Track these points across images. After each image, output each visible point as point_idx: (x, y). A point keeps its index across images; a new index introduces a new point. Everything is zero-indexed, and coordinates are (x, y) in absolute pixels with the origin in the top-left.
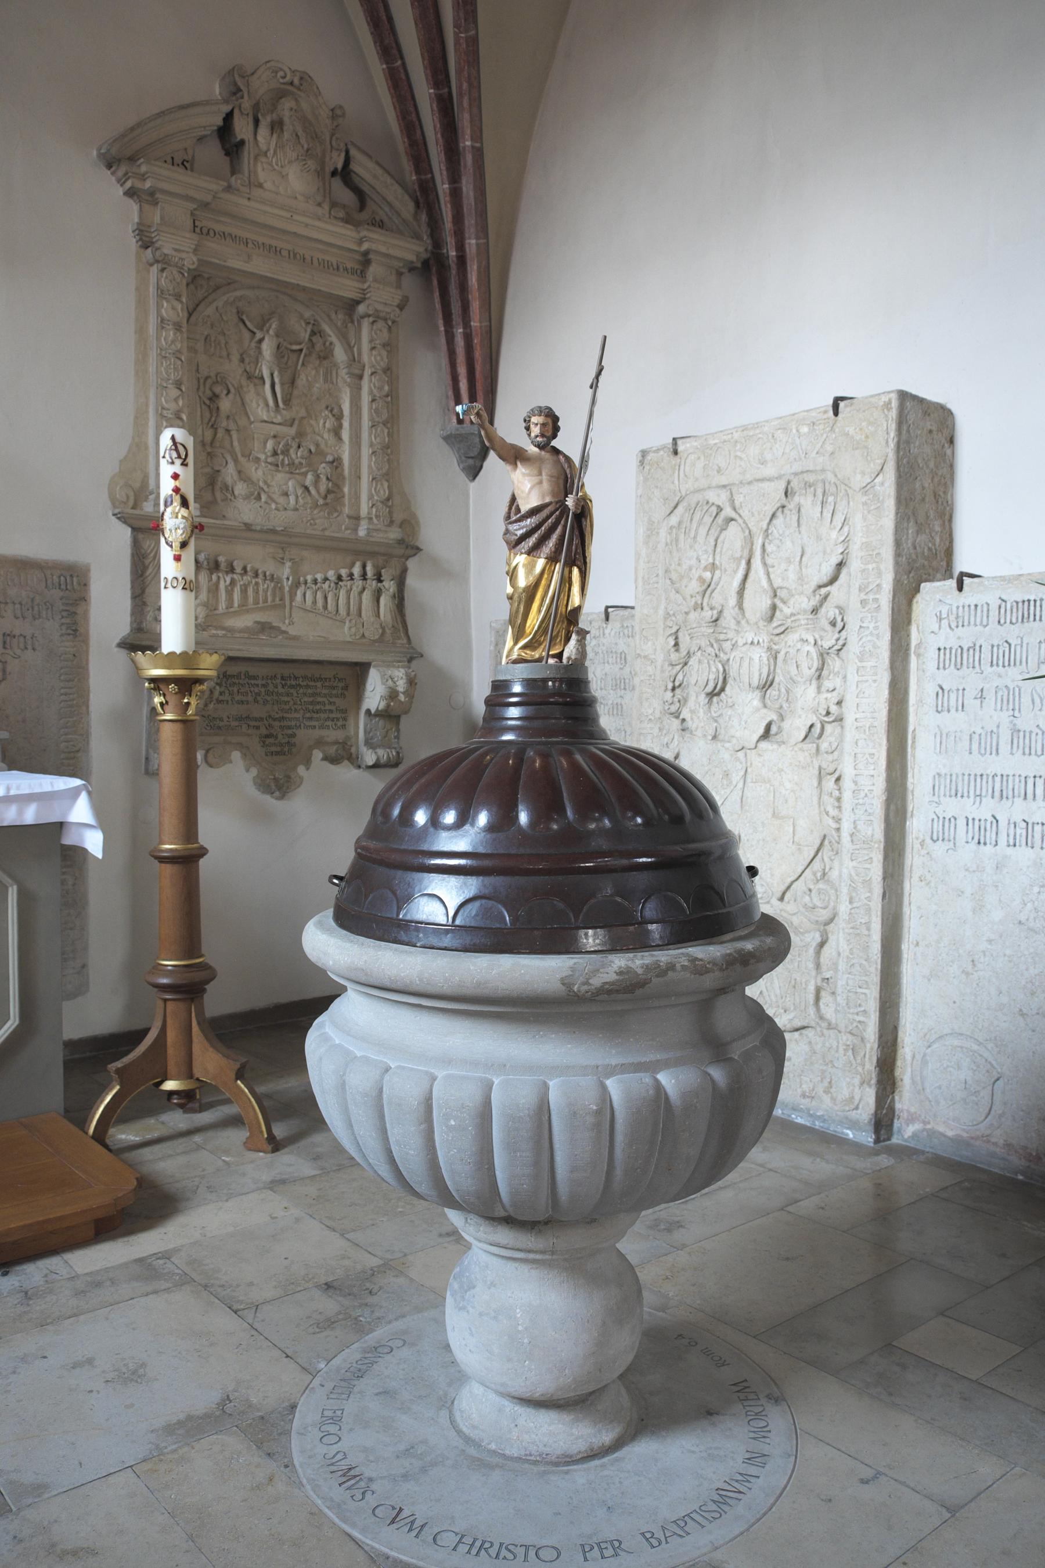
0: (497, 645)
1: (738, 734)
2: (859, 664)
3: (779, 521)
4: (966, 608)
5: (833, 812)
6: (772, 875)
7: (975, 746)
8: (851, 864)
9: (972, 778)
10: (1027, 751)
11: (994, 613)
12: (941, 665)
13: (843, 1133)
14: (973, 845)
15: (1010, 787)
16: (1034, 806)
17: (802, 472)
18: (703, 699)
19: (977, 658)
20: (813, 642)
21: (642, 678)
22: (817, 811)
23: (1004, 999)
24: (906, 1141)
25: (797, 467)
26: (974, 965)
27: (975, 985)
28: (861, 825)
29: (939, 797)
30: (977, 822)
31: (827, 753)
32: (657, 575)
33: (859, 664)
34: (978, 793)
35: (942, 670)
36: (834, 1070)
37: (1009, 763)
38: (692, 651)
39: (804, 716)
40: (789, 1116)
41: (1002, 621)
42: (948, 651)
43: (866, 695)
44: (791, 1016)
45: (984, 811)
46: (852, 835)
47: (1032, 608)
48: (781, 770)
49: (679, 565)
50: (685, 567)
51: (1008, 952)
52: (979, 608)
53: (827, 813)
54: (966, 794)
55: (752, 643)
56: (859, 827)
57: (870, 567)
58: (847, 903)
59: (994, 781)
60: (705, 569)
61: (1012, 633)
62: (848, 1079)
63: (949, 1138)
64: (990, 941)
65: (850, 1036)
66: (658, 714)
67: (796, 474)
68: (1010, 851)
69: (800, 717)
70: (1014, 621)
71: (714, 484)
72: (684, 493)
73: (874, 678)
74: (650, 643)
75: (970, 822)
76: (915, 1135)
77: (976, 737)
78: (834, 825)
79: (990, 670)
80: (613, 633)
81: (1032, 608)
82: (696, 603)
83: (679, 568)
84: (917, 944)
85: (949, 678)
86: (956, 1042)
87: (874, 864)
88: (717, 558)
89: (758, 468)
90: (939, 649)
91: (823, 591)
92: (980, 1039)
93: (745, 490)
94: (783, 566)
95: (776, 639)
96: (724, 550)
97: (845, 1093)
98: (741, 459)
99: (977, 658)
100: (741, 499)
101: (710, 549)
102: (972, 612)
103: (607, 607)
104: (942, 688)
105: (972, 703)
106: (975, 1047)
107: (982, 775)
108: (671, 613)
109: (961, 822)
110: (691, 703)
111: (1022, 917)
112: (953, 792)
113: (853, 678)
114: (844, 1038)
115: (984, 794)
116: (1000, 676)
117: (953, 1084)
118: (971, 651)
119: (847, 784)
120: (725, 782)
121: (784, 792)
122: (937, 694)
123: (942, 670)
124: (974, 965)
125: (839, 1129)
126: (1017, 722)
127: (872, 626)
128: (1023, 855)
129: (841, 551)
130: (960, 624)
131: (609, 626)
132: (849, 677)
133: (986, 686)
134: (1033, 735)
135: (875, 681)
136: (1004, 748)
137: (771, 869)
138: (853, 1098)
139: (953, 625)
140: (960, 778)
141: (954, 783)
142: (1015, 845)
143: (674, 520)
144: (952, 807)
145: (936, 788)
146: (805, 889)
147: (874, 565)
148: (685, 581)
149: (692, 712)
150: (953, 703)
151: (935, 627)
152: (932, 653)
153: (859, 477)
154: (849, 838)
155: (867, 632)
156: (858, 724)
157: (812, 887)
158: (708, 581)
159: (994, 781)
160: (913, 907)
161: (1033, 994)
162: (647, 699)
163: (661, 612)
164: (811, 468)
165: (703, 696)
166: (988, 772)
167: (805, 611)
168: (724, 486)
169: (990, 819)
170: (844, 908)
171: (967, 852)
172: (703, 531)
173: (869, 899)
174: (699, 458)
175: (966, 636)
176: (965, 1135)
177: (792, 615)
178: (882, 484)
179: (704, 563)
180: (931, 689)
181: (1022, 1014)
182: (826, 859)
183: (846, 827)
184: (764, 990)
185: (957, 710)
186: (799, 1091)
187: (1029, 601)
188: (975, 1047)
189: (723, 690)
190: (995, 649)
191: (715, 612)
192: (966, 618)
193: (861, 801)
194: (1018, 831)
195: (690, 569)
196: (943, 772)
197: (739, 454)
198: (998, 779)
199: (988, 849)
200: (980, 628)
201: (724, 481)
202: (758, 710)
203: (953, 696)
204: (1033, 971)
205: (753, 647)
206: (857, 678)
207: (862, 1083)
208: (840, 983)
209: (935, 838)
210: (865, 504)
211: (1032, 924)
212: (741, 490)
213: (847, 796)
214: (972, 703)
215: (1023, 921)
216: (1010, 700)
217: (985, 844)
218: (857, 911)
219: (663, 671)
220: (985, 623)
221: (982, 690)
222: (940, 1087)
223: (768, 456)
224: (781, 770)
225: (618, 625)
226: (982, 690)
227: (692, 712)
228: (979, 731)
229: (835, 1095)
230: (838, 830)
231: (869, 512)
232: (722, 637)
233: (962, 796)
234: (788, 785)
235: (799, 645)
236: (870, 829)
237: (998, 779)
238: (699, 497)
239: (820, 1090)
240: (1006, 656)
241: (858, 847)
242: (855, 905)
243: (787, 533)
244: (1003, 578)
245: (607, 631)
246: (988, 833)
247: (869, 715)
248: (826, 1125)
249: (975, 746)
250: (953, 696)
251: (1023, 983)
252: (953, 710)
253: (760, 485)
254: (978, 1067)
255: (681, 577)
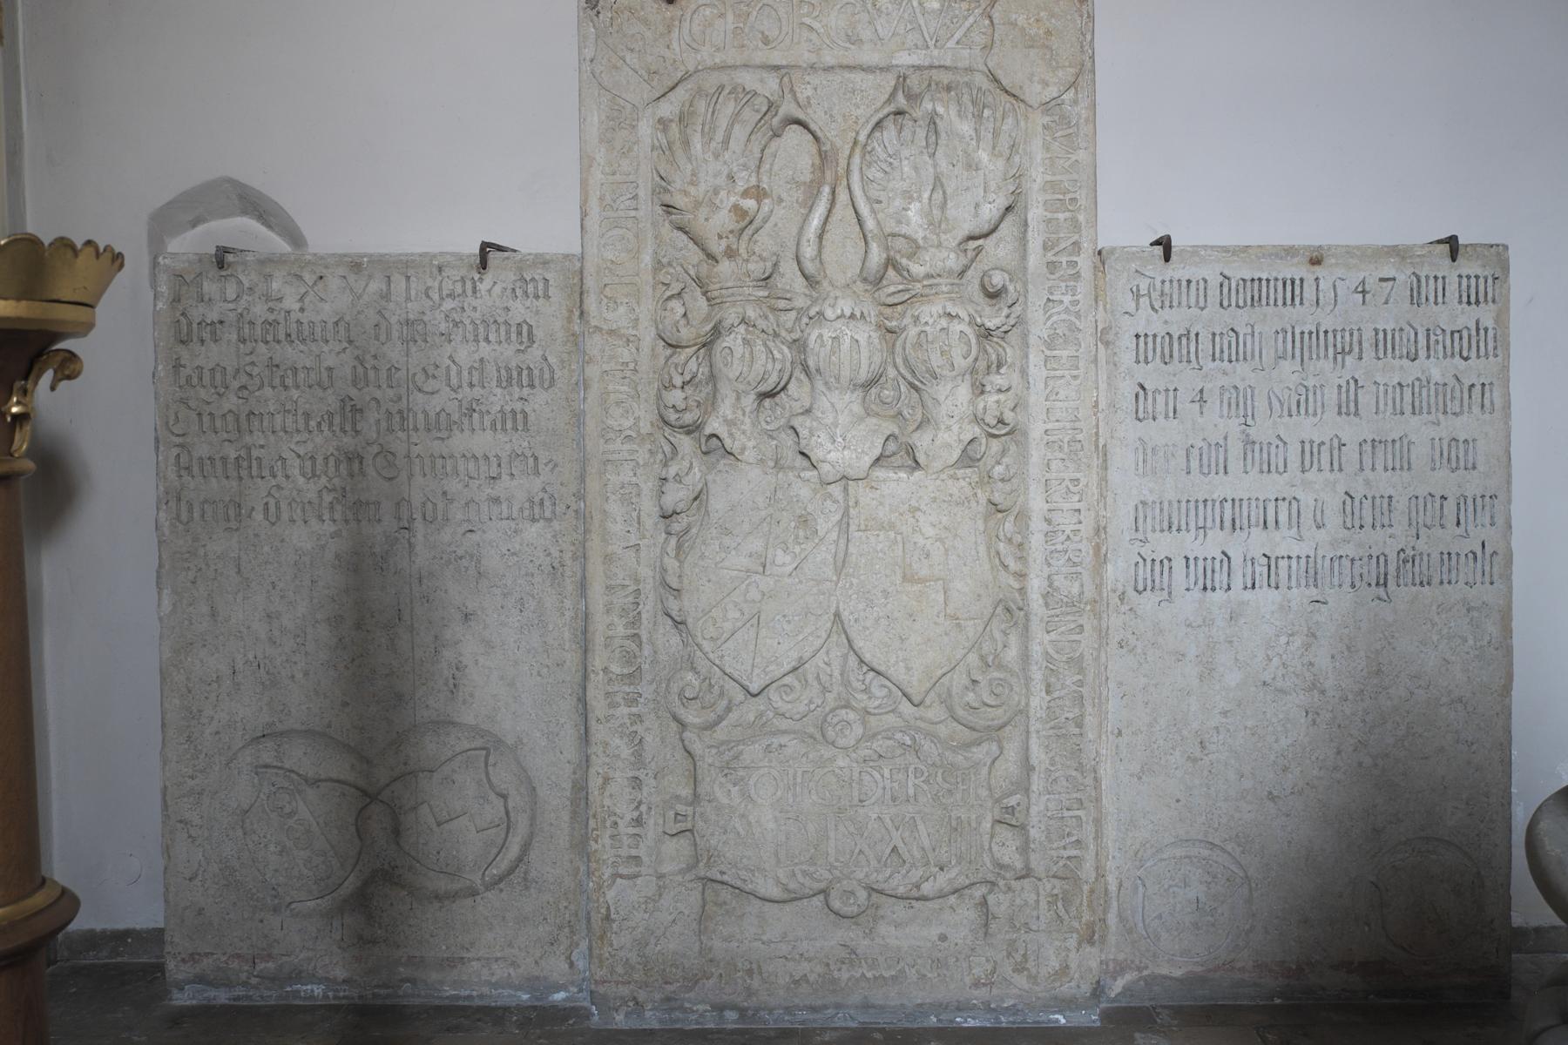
0: (177, 299)
1: (832, 456)
2: (1048, 353)
3: (889, 133)
4: (1175, 284)
5: (1013, 565)
6: (908, 669)
7: (1194, 464)
8: (1047, 637)
9: (1192, 505)
10: (1265, 468)
11: (1214, 293)
12: (1142, 358)
13: (1050, 1021)
14: (1197, 593)
15: (1245, 514)
16: (1277, 536)
17: (931, 67)
18: (749, 401)
19: (1193, 349)
20: (967, 319)
21: (606, 367)
22: (987, 567)
23: (1248, 784)
24: (1113, 1000)
25: (915, 59)
26: (1203, 748)
27: (1206, 773)
28: (1059, 581)
29: (1145, 532)
30: (1201, 563)
31: (1002, 480)
32: (635, 197)
33: (1048, 353)
34: (1201, 524)
35: (1142, 364)
36: (1031, 935)
37: (1242, 484)
38: (727, 324)
39: (955, 428)
40: (952, 1021)
41: (1225, 303)
42: (1150, 339)
43: (1061, 396)
44: (953, 874)
45: (1212, 545)
46: (1046, 596)
47: (1264, 290)
48: (914, 510)
49: (692, 183)
50: (703, 187)
51: (1250, 724)
52: (1193, 285)
53: (1006, 567)
54: (1184, 527)
55: (852, 316)
56: (1056, 584)
57: (1061, 216)
58: (1043, 694)
59: (1222, 507)
60: (746, 194)
61: (1241, 319)
62: (1057, 943)
63: (1176, 979)
64: (1225, 713)
65: (1055, 881)
66: (645, 428)
67: (918, 68)
68: (1248, 595)
69: (949, 428)
70: (1241, 303)
71: (758, 61)
72: (691, 69)
73: (1075, 373)
74: (622, 310)
75: (1192, 562)
76: (1126, 989)
77: (1195, 452)
78: (1017, 586)
79: (1211, 365)
80: (497, 289)
81: (1264, 290)
82: (728, 246)
83: (692, 190)
84: (1120, 733)
85: (1153, 374)
86: (1179, 852)
87: (1086, 634)
88: (765, 179)
89: (847, 49)
90: (1137, 336)
91: (973, 244)
92: (1217, 842)
93: (815, 79)
94: (898, 203)
95: (888, 311)
96: (776, 168)
97: (1054, 964)
98: (811, 28)
99: (1193, 349)
100: (809, 92)
101: (753, 165)
102: (1184, 289)
103: (485, 247)
104: (1143, 387)
105: (1187, 408)
106: (1206, 853)
107: (1205, 501)
108: (665, 261)
109: (1179, 564)
110: (726, 408)
111: (1267, 677)
112: (1166, 524)
113: (1037, 371)
114: (1049, 886)
115: (1209, 524)
116: (1225, 373)
117: (1179, 907)
118: (1184, 341)
119: (1037, 525)
120: (801, 533)
121: (921, 541)
122: (1137, 396)
123: (1142, 364)
124: (1203, 748)
125: (1043, 1017)
126: (1251, 431)
127: (1067, 299)
128: (1266, 598)
129: (1012, 188)
130: (1167, 303)
131: (489, 278)
132: (1032, 370)
133: (1208, 386)
134: (1273, 449)
135: (1075, 377)
136: (1235, 465)
137: (904, 660)
138: (1067, 967)
139: (1157, 305)
140: (1176, 505)
141: (1166, 514)
142: (1253, 586)
143: (667, 109)
144: (1163, 545)
145: (1141, 521)
146: (965, 681)
147: (1068, 214)
148: (703, 212)
149: (730, 423)
150: (1160, 407)
151: (1131, 306)
152: (1127, 341)
153: (1038, 87)
154: (1041, 601)
155: (1060, 308)
156: (1051, 438)
157: (979, 678)
158: (751, 213)
159: (1222, 507)
160: (1112, 685)
161: (1285, 769)
162: (618, 404)
163: (647, 259)
164: (948, 63)
165: (752, 396)
166: (1215, 496)
167: (950, 272)
168: (777, 68)
169: (1219, 556)
170: (1038, 702)
171: (1188, 603)
172: (740, 133)
173: (1081, 683)
174: (722, 15)
175: (1177, 320)
176: (1200, 969)
177: (929, 276)
178: (1075, 102)
179: (741, 186)
180: (1127, 389)
181: (1271, 797)
182: (997, 635)
183: (1036, 584)
184: (900, 845)
185: (1167, 417)
186: (968, 980)
187: (1260, 280)
188: (1206, 853)
189: (784, 388)
190: (1217, 339)
191: (769, 264)
192: (1175, 297)
193: (1059, 547)
194: (1258, 569)
195: (716, 192)
196: (1150, 499)
197: (807, 21)
198: (1228, 505)
199: (1218, 596)
200: (1194, 311)
201: (777, 58)
202: (861, 419)
203: (1161, 399)
204: (1284, 742)
205: (852, 323)
206: (1045, 373)
207: (1080, 944)
208: (1034, 810)
209: (1141, 588)
210: (1045, 127)
211: (1280, 683)
212: (807, 78)
213: (1036, 541)
214: (1187, 408)
215: (1269, 681)
216: (1239, 402)
217: (1213, 589)
218: (1060, 702)
219: (654, 356)
220: (1202, 304)
221: (1201, 391)
222: (1160, 917)
223: (866, 34)
224: (914, 510)
225: (512, 276)
226: (1201, 391)
227: (730, 423)
228: (1200, 444)
229: (1034, 971)
230: (1022, 590)
231: (1054, 139)
232: (782, 304)
233: (1179, 530)
234: (930, 532)
235: (944, 322)
236: (1077, 584)
237: (1228, 505)
238: (724, 78)
239: (1007, 969)
240: (1231, 349)
241: (1058, 611)
242: (1056, 694)
243: (905, 153)
244: (1225, 249)
245: (482, 288)
246: (1217, 575)
247: (1068, 425)
248: (1019, 1019)
249: (1194, 464)
250: (1161, 399)
251: (1272, 758)
252: (1161, 418)
253: (847, 75)
254: (1215, 877)
255: (698, 204)
